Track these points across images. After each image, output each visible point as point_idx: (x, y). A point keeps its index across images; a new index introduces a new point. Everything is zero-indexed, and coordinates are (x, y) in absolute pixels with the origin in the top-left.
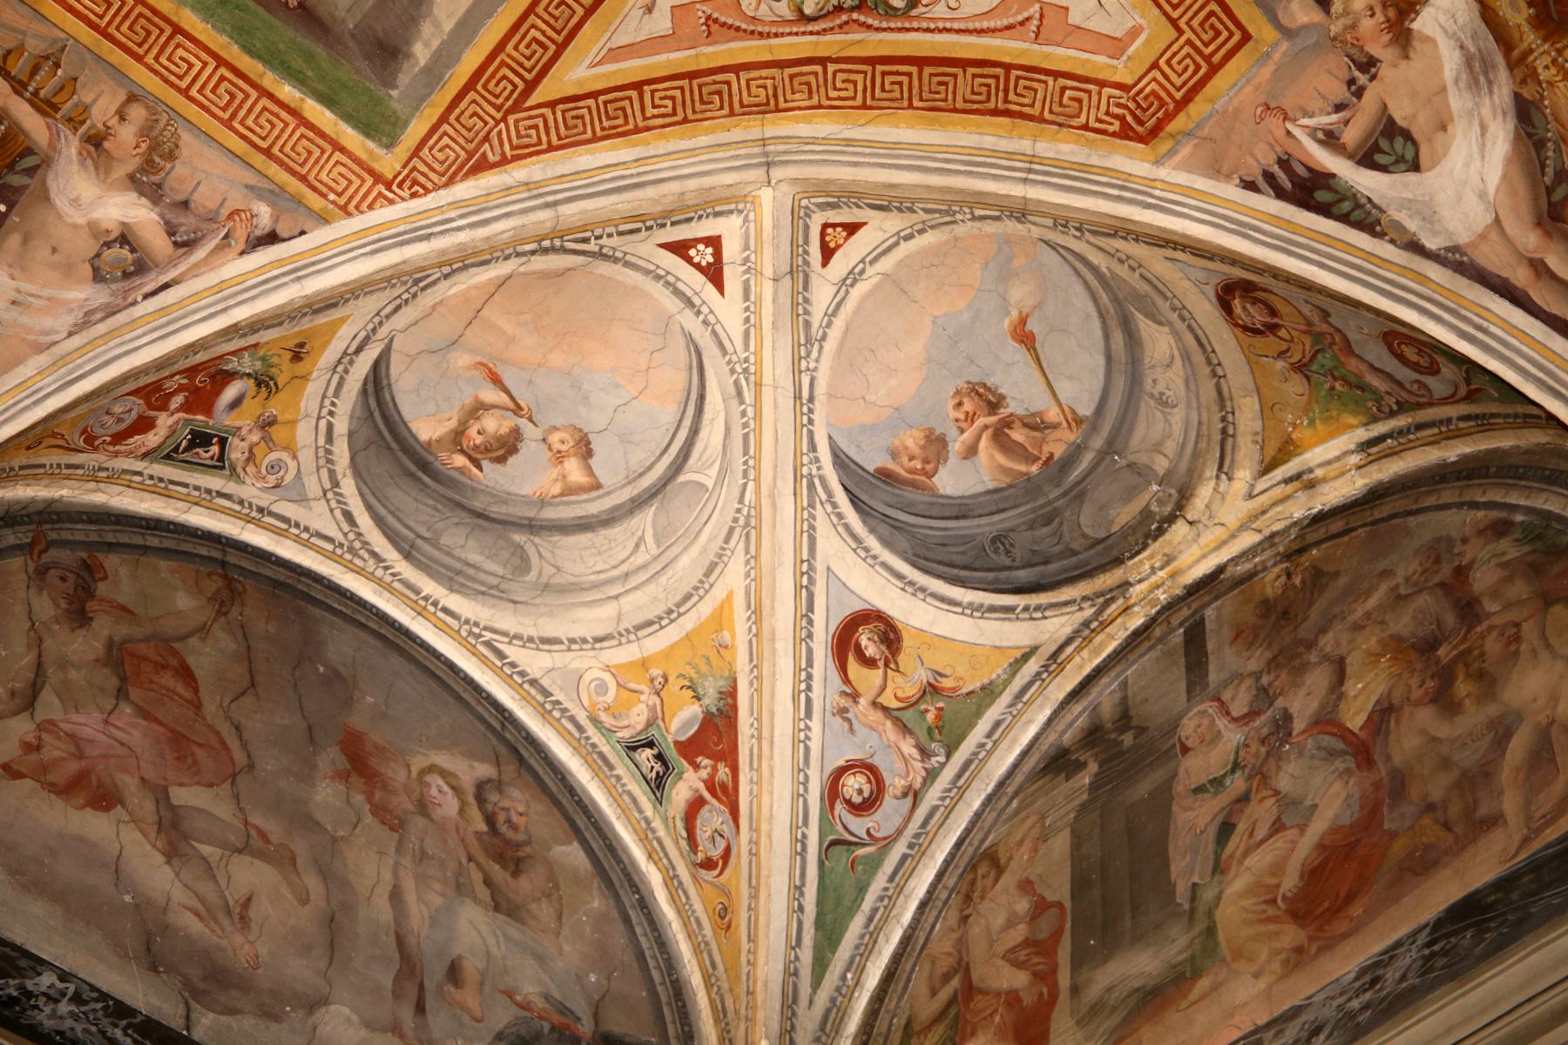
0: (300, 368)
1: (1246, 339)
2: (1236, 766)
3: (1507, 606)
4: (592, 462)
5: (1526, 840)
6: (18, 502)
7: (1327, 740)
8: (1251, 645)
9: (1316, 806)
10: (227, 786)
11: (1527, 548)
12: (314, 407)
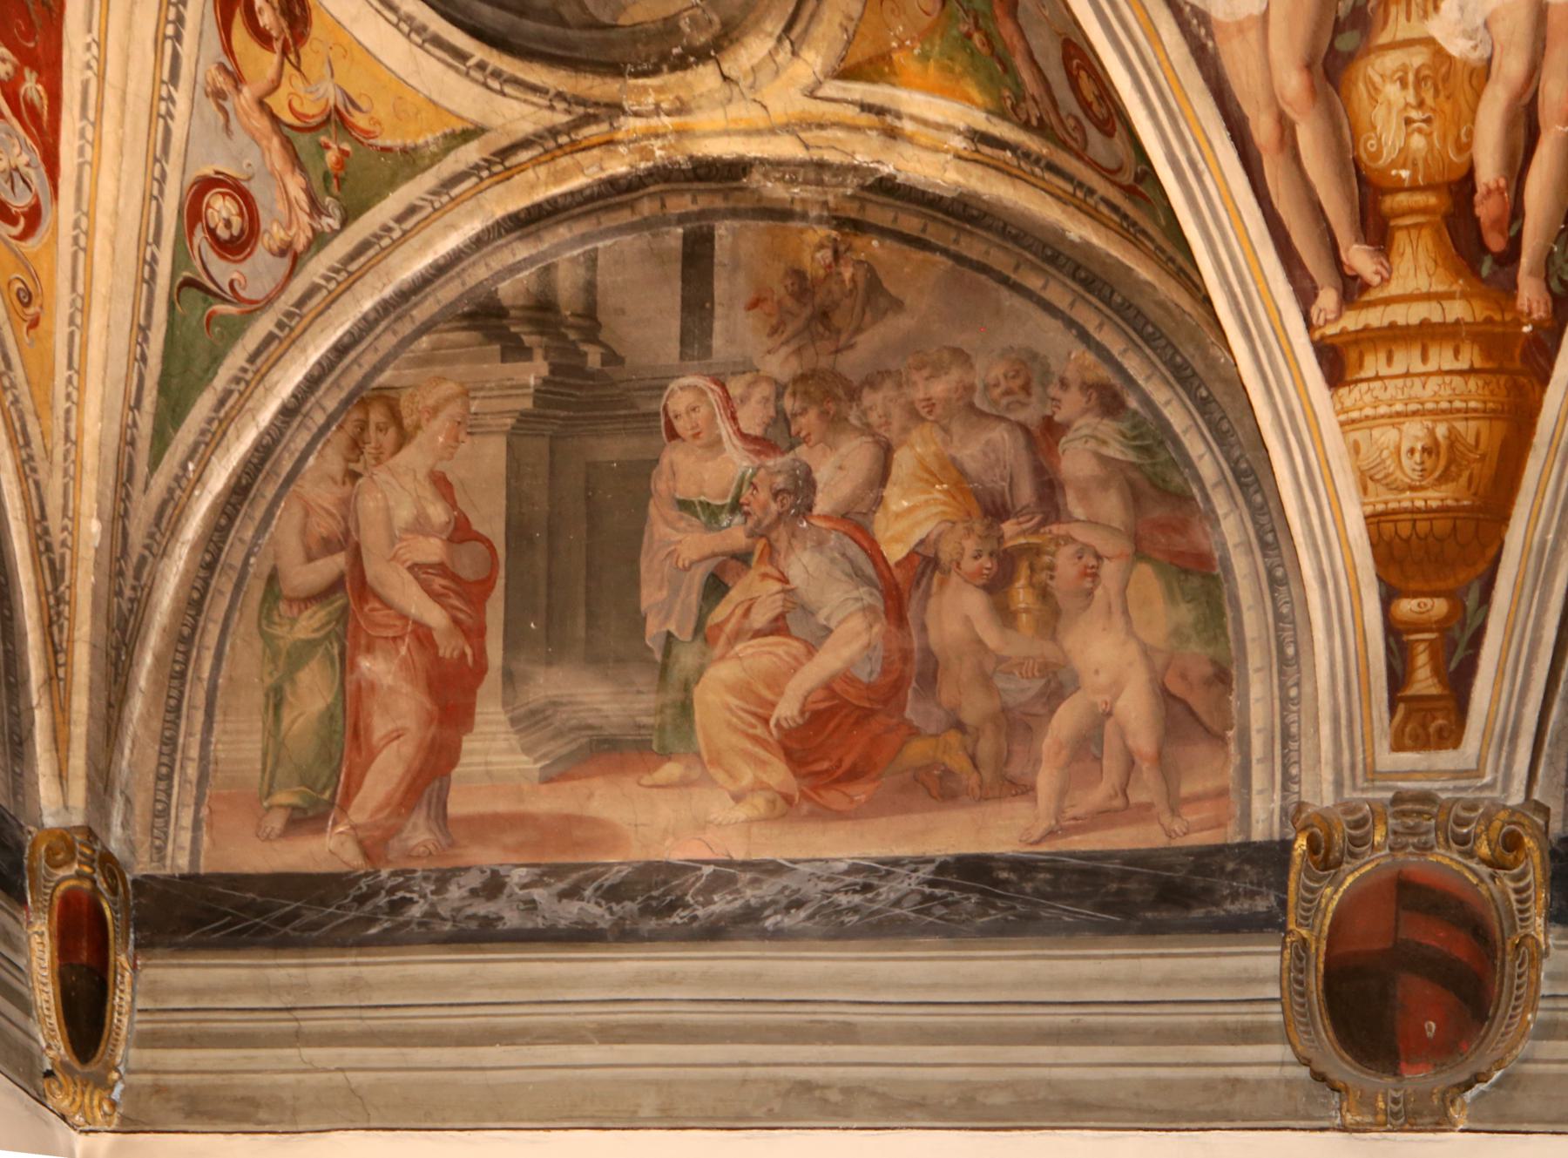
2: (736, 507)
3: (1092, 522)
5: (1051, 834)
7: (853, 550)
8: (774, 331)
9: (828, 631)
11: (1132, 457)
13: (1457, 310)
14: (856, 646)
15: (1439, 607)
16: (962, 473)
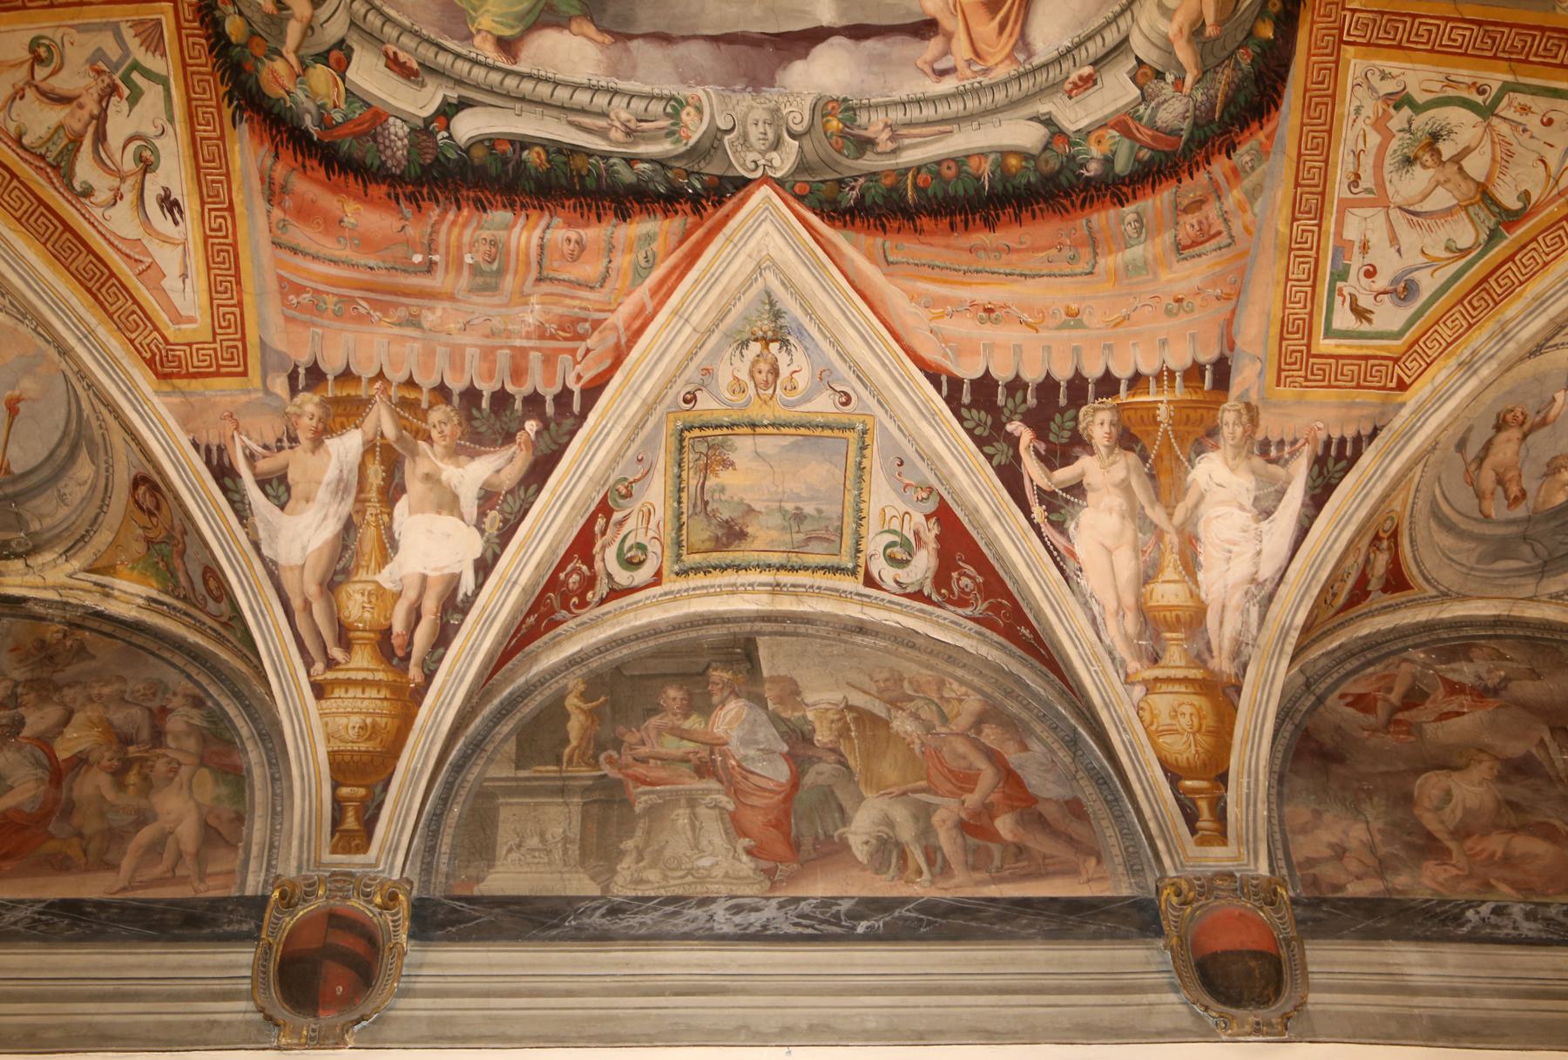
1: (133, 506)
5: (124, 889)
7: (39, 753)
8: (21, 661)
9: (12, 788)
13: (380, 676)
14: (27, 795)
15: (362, 792)
16: (111, 724)
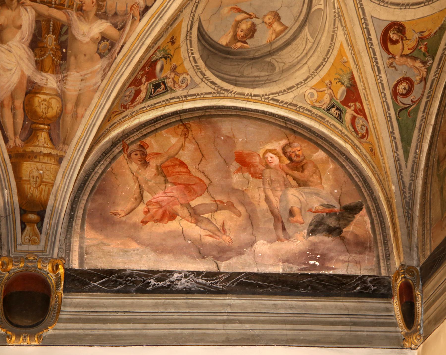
0: (176, 45)
4: (281, 21)
6: (114, 137)
10: (206, 193)
12: (186, 55)
